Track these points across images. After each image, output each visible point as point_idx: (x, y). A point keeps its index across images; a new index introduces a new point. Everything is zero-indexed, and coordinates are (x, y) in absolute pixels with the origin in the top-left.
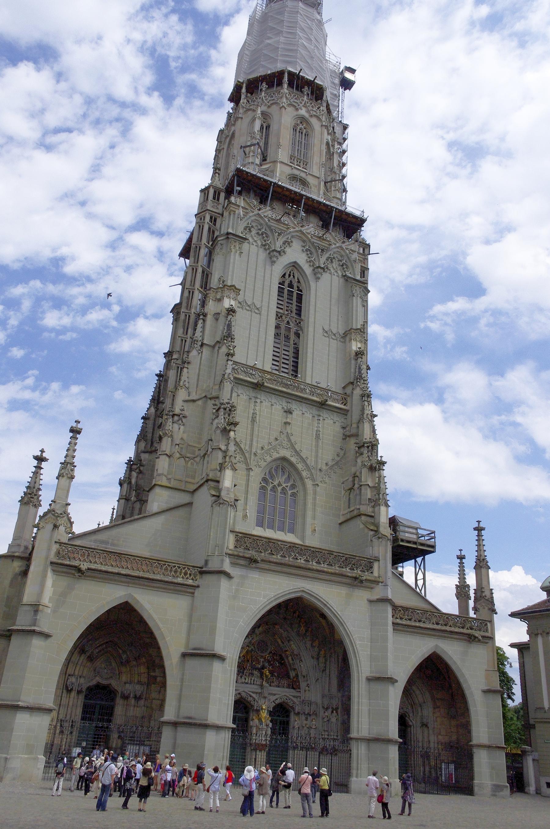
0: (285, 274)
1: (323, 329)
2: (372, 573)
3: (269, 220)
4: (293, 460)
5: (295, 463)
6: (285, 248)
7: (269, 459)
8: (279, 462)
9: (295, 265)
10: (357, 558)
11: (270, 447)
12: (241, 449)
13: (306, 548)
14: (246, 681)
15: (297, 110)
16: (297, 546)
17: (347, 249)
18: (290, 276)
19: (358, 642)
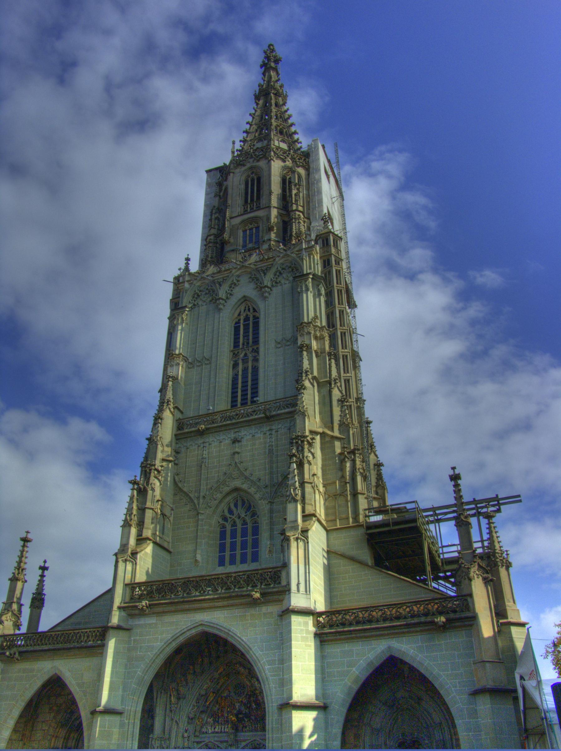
0: (240, 312)
1: (276, 342)
2: (280, 583)
3: (212, 277)
4: (245, 486)
5: (246, 488)
6: (232, 291)
7: (219, 496)
8: (235, 494)
9: (245, 299)
10: (260, 572)
11: (219, 484)
12: (190, 498)
13: (201, 578)
14: (216, 730)
15: (244, 165)
16: (192, 579)
17: (292, 253)
18: (245, 310)
19: (267, 667)
